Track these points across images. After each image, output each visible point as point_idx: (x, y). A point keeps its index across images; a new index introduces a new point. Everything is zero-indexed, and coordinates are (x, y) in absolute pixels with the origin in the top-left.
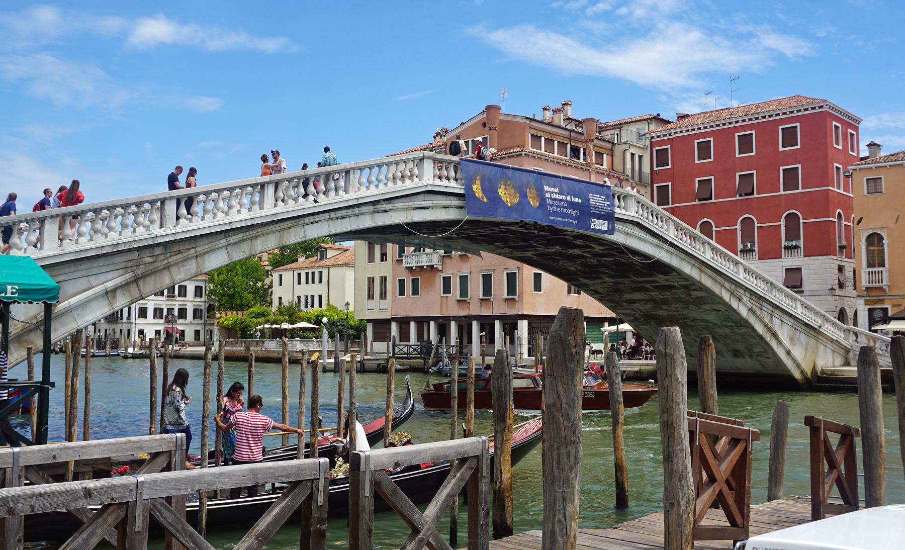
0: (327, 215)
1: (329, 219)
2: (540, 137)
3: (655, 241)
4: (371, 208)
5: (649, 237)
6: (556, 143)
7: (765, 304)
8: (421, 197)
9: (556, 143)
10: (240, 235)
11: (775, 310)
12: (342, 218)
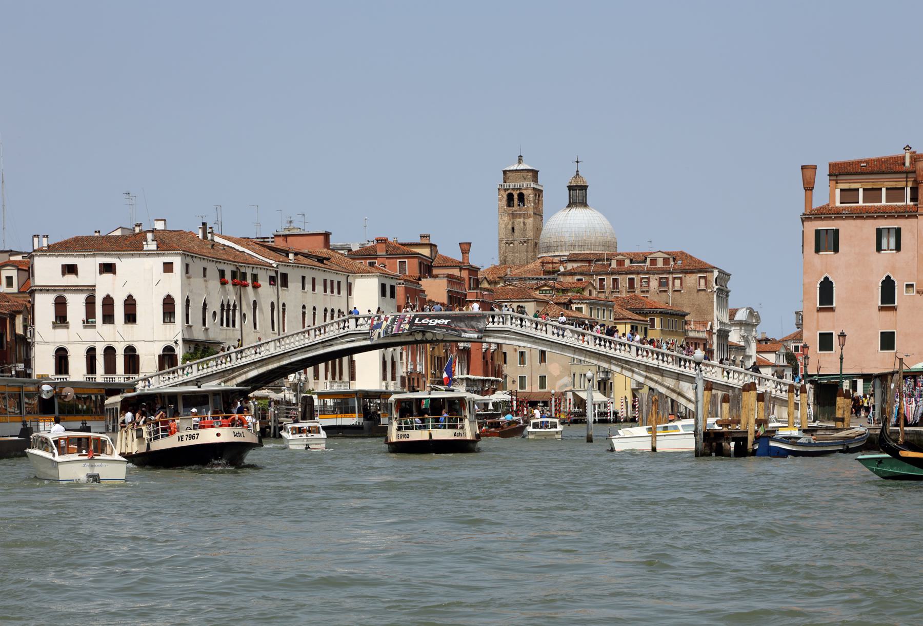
0: (298, 351)
1: (301, 352)
2: (857, 190)
3: (530, 339)
4: (320, 345)
5: (525, 338)
6: (884, 190)
7: (665, 372)
8: (349, 336)
9: (884, 190)
10: (260, 364)
11: (680, 376)
12: (308, 351)
